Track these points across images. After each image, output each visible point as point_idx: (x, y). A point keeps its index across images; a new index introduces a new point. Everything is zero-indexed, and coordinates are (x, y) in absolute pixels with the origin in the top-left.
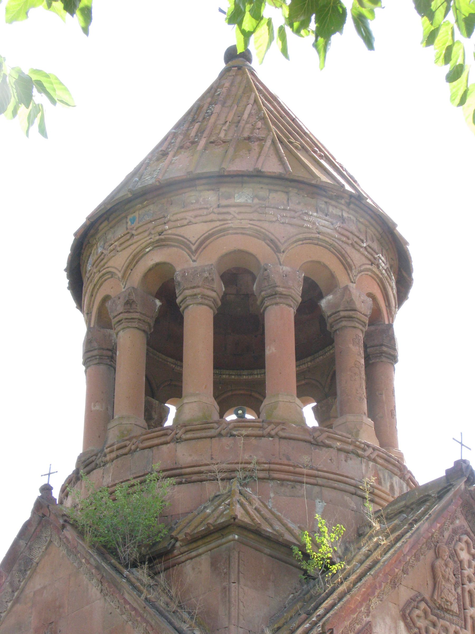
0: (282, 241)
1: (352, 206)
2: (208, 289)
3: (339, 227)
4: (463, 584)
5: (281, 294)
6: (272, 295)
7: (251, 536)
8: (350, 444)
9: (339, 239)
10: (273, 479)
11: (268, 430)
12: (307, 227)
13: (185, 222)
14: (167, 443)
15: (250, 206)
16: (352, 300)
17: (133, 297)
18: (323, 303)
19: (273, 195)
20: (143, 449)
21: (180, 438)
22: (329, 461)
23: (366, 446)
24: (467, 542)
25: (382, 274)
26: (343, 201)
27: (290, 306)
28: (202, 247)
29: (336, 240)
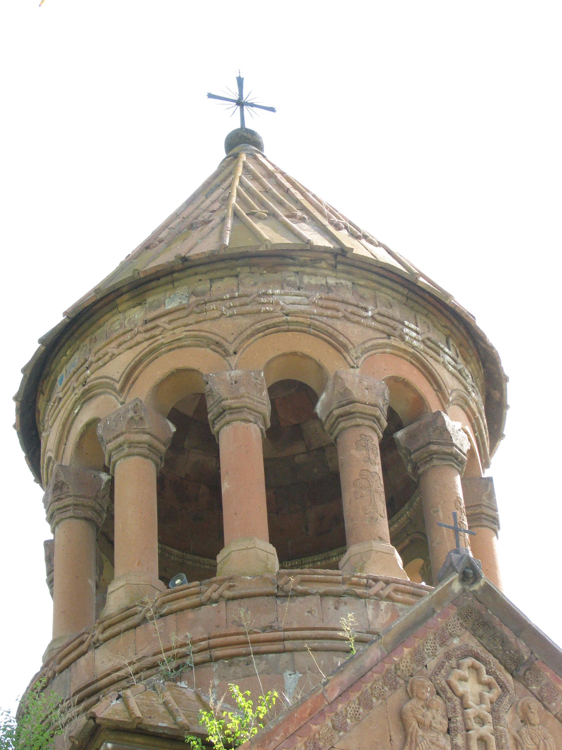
0: (231, 339)
1: (339, 267)
2: (137, 433)
3: (321, 298)
4: (468, 730)
5: (231, 408)
6: (221, 414)
7: (138, 739)
8: (344, 582)
9: (321, 315)
10: (217, 659)
11: (208, 593)
12: (266, 312)
13: (107, 358)
14: (84, 653)
15: (184, 308)
16: (346, 389)
17: (62, 478)
18: (319, 409)
19: (217, 285)
20: (61, 671)
21: (98, 640)
22: (306, 614)
23: (370, 581)
24: (473, 667)
25: (413, 347)
26: (323, 264)
27: (247, 421)
28: (131, 382)
29: (317, 317)
